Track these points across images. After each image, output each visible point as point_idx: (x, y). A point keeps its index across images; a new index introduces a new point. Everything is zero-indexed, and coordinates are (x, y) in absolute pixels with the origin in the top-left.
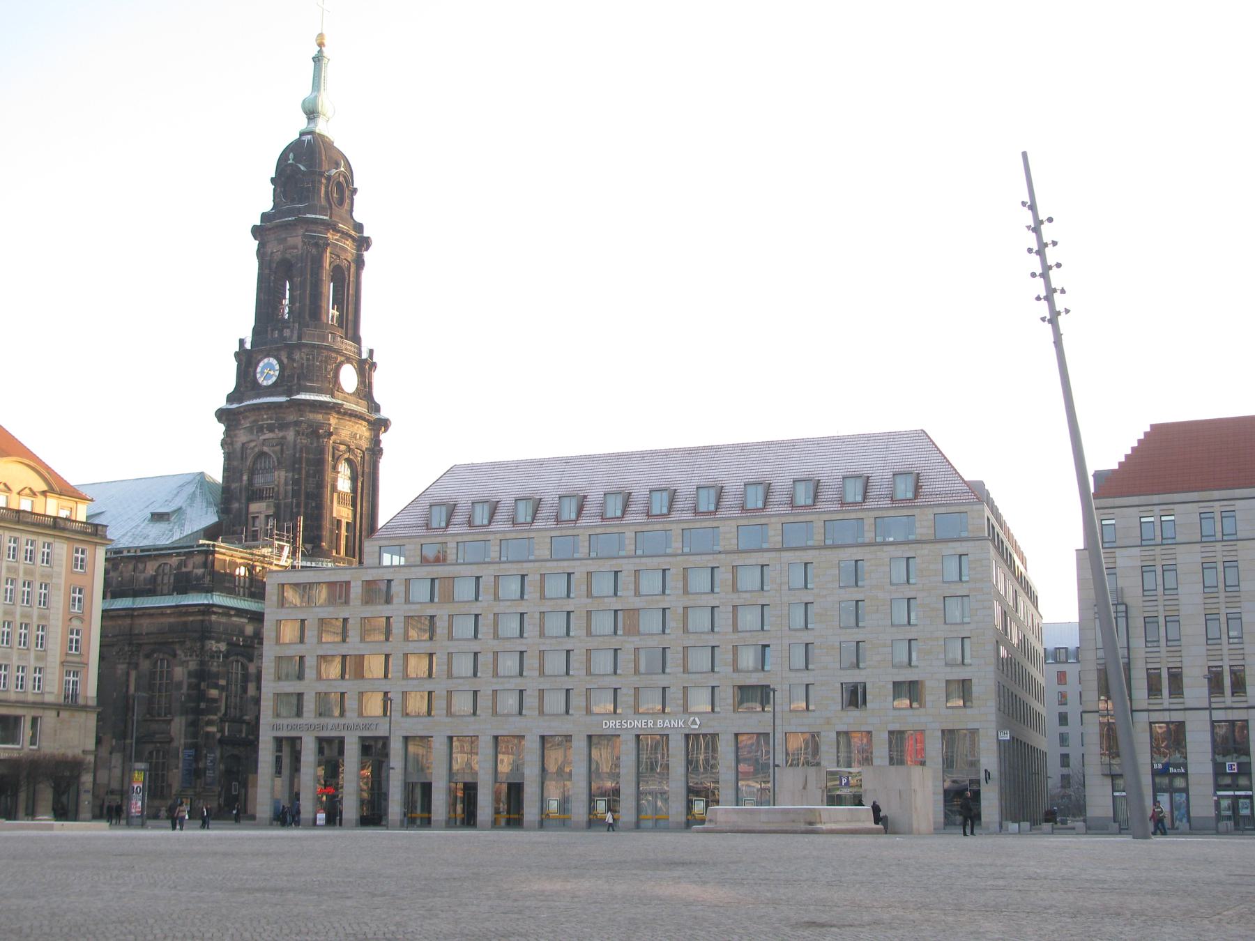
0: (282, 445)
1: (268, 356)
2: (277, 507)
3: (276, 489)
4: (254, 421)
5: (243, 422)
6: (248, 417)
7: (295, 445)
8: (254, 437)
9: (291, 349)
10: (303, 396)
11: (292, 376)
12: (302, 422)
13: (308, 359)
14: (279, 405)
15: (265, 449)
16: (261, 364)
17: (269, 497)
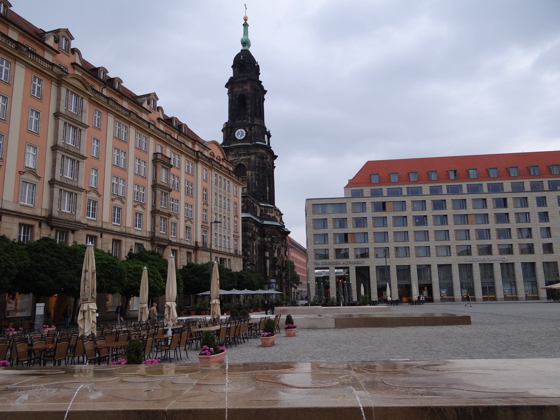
0: (249, 161)
1: (240, 128)
2: (248, 184)
3: (247, 177)
4: (237, 152)
5: (230, 153)
6: (233, 151)
7: (255, 161)
8: (237, 158)
9: (250, 126)
10: (257, 143)
11: (251, 137)
12: (258, 152)
13: (257, 130)
14: (248, 146)
15: (242, 163)
16: (237, 131)
17: (244, 181)
